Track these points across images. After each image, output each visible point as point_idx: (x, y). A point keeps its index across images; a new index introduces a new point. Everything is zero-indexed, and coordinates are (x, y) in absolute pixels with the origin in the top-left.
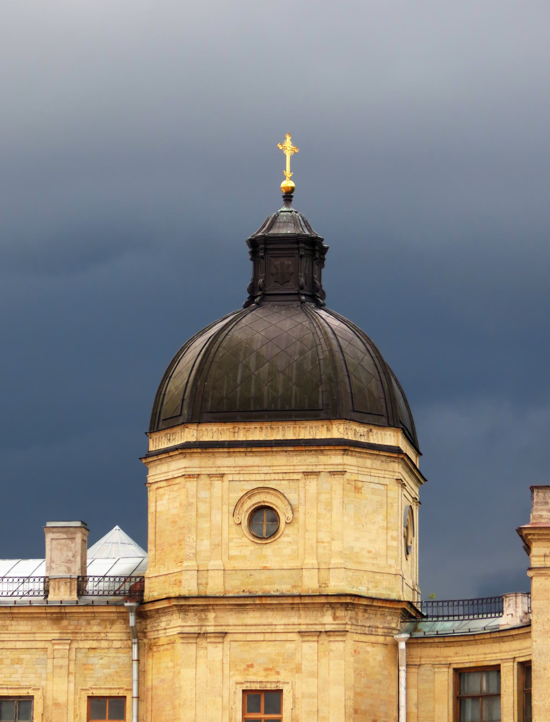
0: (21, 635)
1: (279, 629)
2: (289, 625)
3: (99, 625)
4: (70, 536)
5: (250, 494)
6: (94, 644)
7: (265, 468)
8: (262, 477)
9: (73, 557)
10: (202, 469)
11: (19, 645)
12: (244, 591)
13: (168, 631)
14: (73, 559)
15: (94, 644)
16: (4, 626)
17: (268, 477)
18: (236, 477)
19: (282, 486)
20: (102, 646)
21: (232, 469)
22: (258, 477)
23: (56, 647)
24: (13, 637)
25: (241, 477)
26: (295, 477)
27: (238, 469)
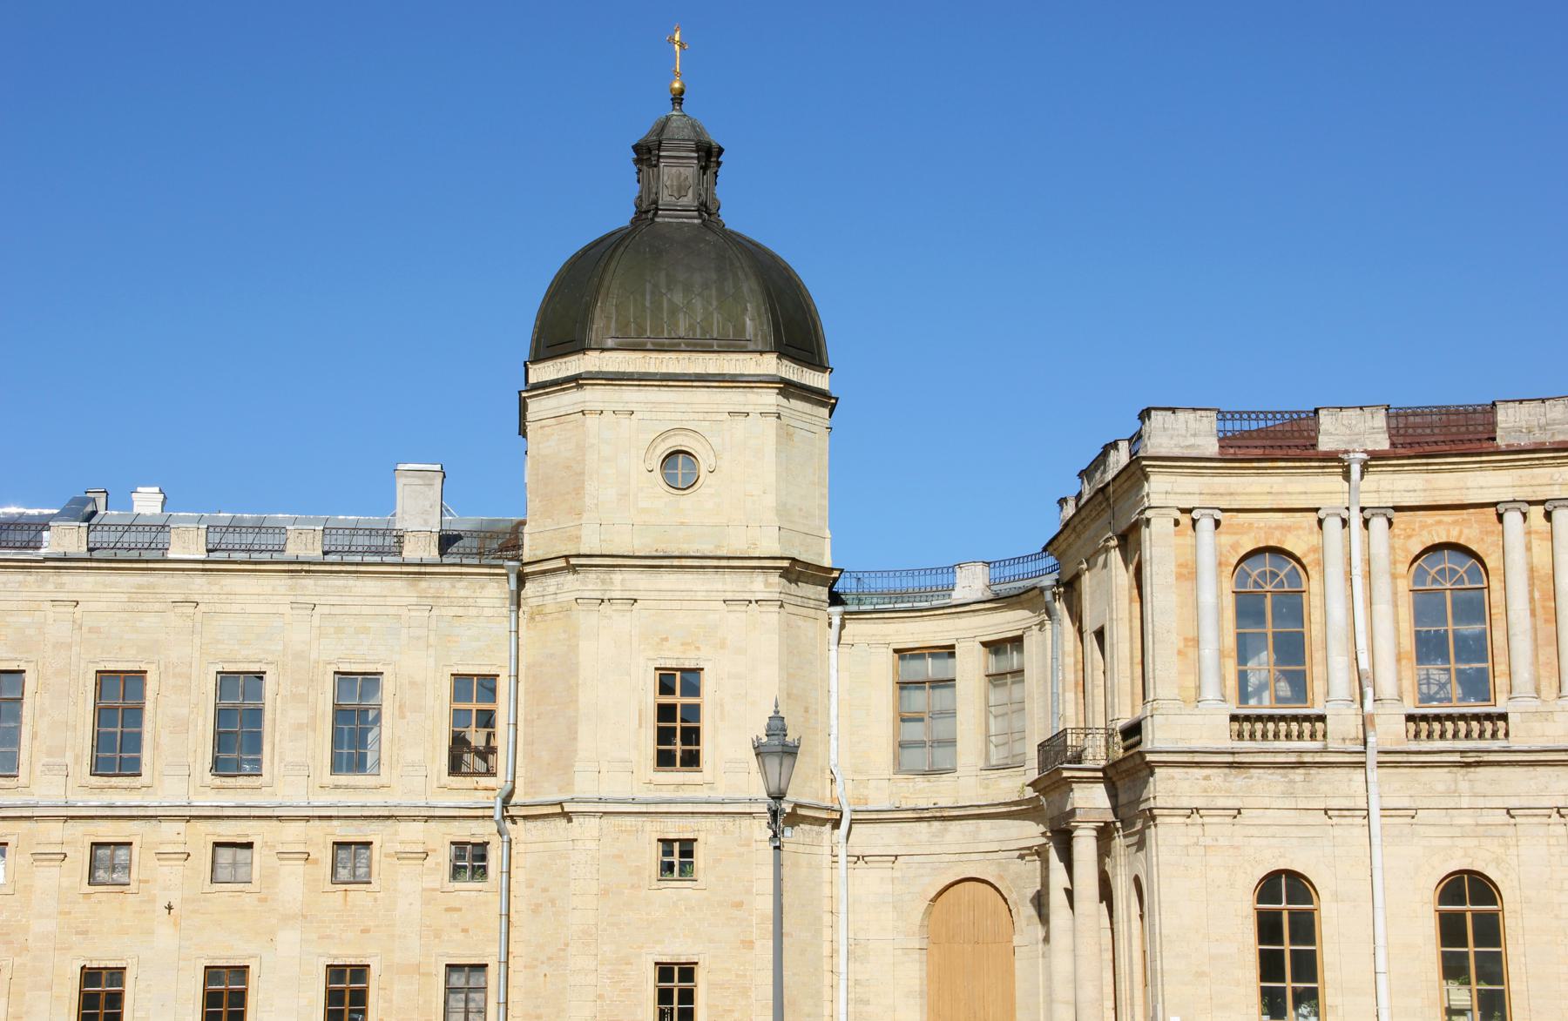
0: (368, 599)
1: (700, 596)
2: (712, 591)
3: (466, 588)
4: (427, 482)
5: (664, 435)
6: (460, 611)
7: (684, 406)
8: (679, 416)
9: (431, 507)
10: (606, 404)
11: (366, 610)
12: (657, 550)
13: (559, 596)
14: (431, 510)
15: (460, 611)
16: (346, 587)
17: (685, 417)
18: (647, 416)
19: (702, 427)
20: (470, 614)
21: (642, 405)
22: (673, 417)
23: (413, 613)
24: (358, 601)
25: (654, 416)
26: (719, 417)
27: (650, 405)
